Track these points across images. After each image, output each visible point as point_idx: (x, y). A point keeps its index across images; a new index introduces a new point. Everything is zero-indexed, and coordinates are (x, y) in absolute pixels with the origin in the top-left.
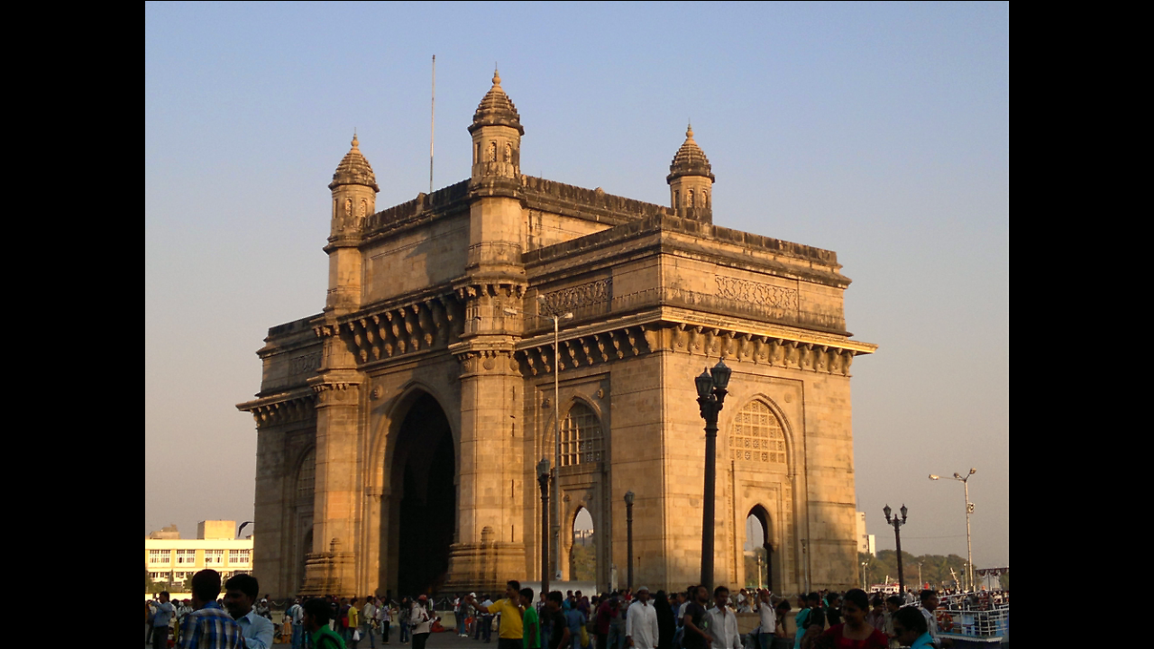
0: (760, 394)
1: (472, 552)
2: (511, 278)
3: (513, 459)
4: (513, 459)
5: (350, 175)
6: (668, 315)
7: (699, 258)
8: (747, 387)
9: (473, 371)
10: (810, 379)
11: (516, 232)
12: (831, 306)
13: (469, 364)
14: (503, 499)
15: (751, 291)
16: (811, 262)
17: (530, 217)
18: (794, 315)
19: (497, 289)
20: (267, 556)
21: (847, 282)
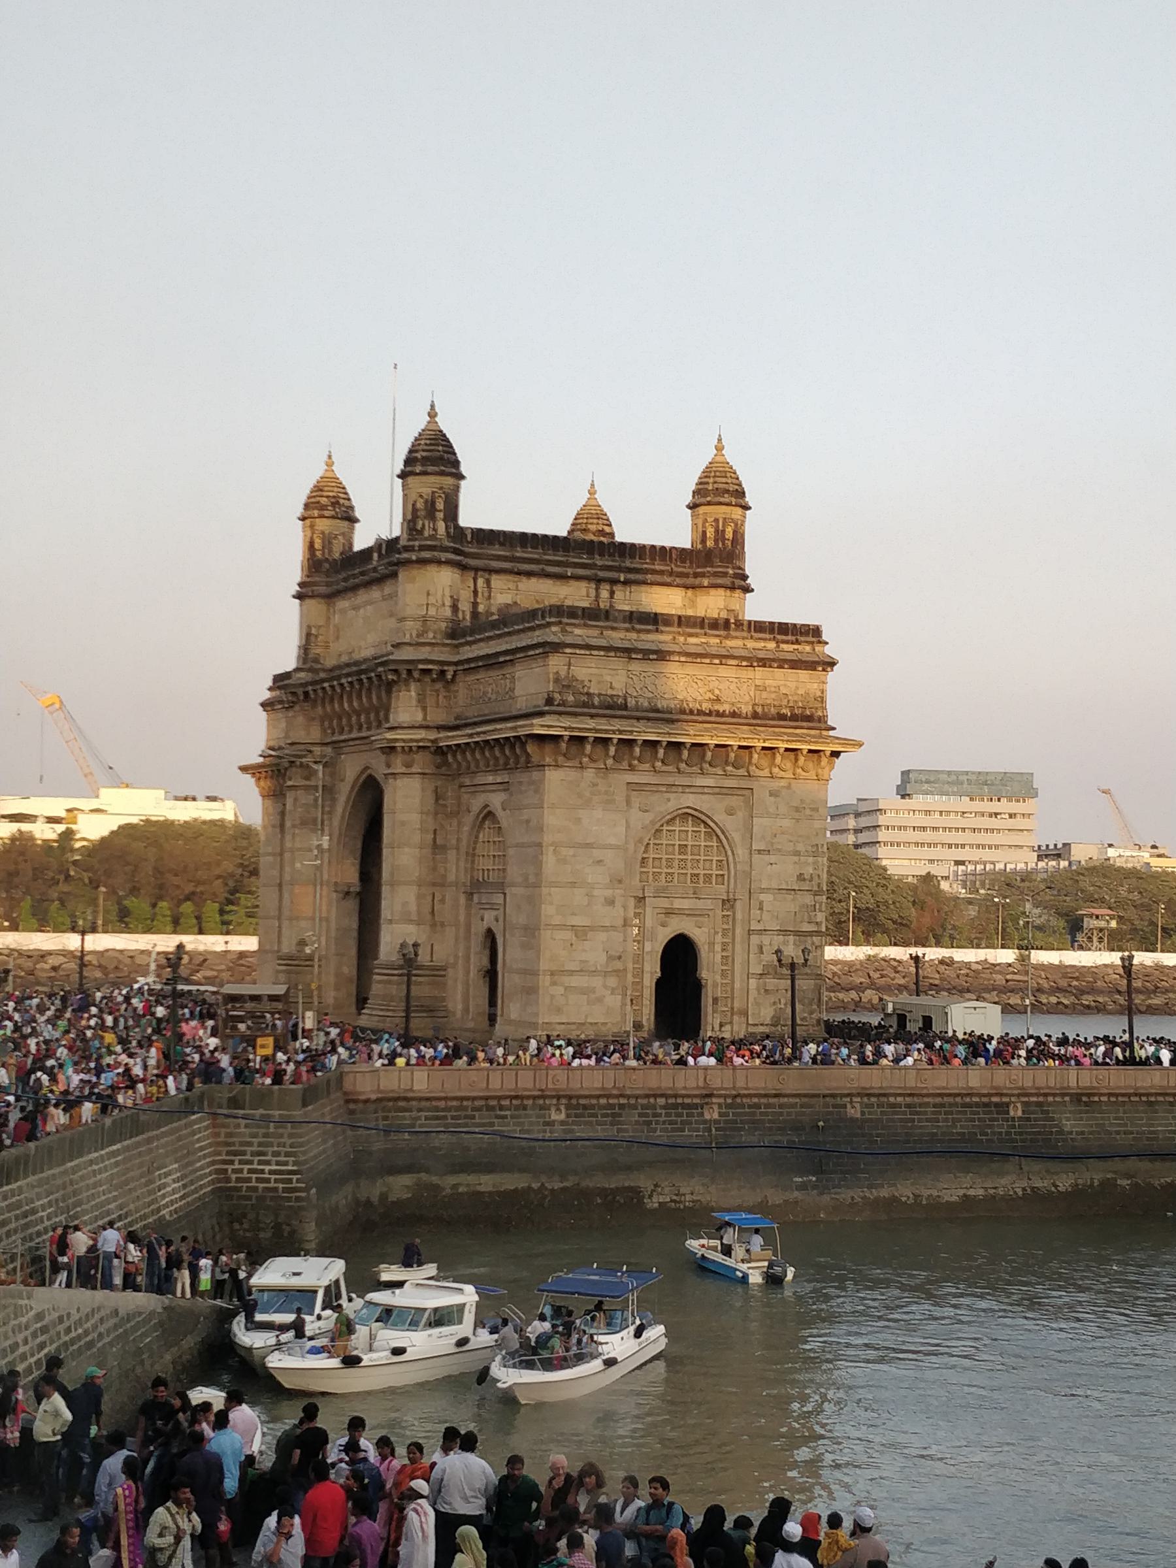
7: (602, 653)
8: (669, 800)
11: (448, 602)
18: (746, 709)
19: (416, 674)
20: (268, 947)
21: (832, 664)
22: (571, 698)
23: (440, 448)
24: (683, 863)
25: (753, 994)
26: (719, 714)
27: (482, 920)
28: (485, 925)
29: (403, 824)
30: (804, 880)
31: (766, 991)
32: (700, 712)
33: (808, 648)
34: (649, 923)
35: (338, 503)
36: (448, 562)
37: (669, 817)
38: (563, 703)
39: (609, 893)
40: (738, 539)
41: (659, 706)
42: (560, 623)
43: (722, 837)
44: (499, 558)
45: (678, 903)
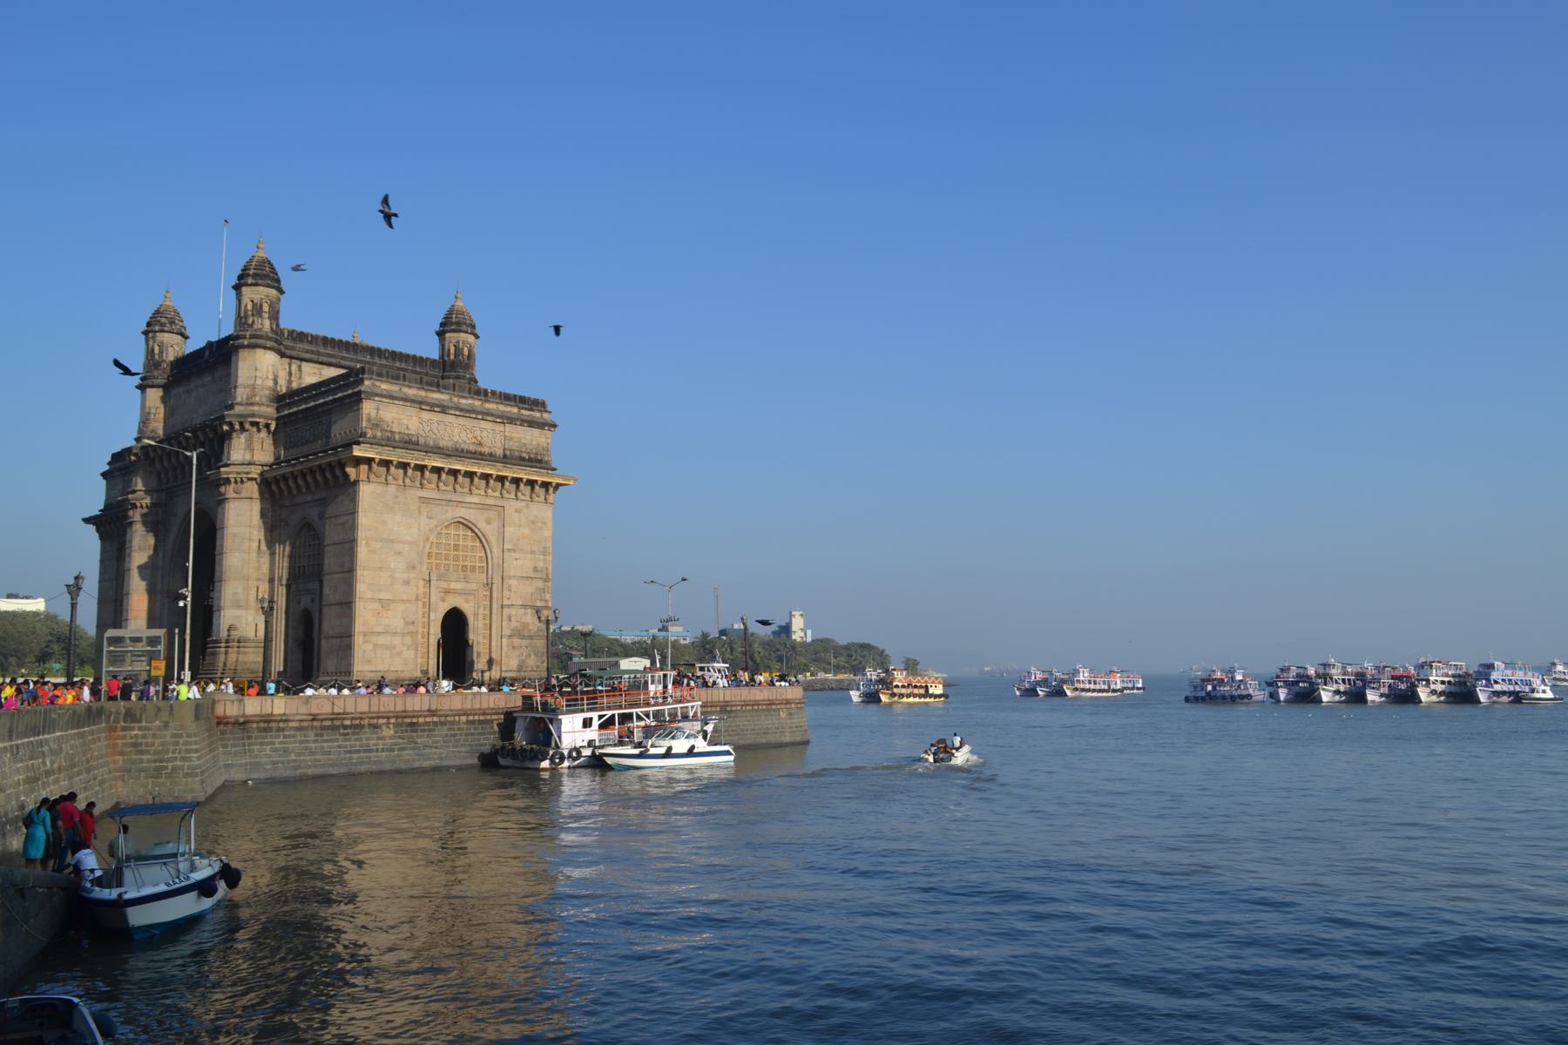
0: (460, 517)
1: (218, 645)
2: (260, 417)
3: (259, 568)
4: (259, 568)
5: (160, 322)
6: (358, 452)
7: (401, 403)
8: (447, 511)
9: (224, 494)
10: (511, 505)
11: (271, 376)
12: (538, 444)
13: (222, 489)
14: (247, 601)
15: (456, 431)
16: (519, 408)
17: (290, 365)
18: (499, 452)
19: (247, 426)
22: (379, 434)
23: (267, 269)
24: (456, 559)
25: (505, 649)
26: (480, 453)
27: (299, 602)
28: (302, 606)
29: (234, 535)
30: (537, 571)
31: (514, 647)
32: (468, 452)
33: (538, 415)
34: (433, 599)
35: (174, 323)
36: (270, 349)
37: (447, 523)
38: (374, 437)
39: (405, 576)
40: (471, 356)
41: (441, 445)
42: (371, 379)
43: (483, 540)
44: (307, 351)
45: (454, 585)
